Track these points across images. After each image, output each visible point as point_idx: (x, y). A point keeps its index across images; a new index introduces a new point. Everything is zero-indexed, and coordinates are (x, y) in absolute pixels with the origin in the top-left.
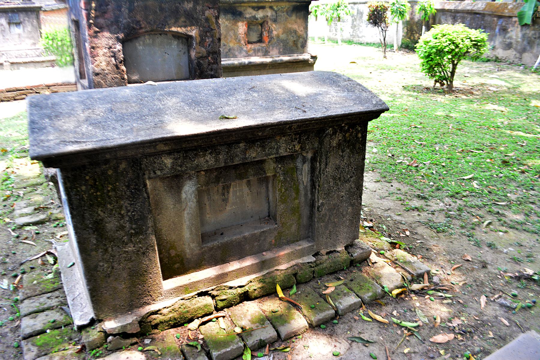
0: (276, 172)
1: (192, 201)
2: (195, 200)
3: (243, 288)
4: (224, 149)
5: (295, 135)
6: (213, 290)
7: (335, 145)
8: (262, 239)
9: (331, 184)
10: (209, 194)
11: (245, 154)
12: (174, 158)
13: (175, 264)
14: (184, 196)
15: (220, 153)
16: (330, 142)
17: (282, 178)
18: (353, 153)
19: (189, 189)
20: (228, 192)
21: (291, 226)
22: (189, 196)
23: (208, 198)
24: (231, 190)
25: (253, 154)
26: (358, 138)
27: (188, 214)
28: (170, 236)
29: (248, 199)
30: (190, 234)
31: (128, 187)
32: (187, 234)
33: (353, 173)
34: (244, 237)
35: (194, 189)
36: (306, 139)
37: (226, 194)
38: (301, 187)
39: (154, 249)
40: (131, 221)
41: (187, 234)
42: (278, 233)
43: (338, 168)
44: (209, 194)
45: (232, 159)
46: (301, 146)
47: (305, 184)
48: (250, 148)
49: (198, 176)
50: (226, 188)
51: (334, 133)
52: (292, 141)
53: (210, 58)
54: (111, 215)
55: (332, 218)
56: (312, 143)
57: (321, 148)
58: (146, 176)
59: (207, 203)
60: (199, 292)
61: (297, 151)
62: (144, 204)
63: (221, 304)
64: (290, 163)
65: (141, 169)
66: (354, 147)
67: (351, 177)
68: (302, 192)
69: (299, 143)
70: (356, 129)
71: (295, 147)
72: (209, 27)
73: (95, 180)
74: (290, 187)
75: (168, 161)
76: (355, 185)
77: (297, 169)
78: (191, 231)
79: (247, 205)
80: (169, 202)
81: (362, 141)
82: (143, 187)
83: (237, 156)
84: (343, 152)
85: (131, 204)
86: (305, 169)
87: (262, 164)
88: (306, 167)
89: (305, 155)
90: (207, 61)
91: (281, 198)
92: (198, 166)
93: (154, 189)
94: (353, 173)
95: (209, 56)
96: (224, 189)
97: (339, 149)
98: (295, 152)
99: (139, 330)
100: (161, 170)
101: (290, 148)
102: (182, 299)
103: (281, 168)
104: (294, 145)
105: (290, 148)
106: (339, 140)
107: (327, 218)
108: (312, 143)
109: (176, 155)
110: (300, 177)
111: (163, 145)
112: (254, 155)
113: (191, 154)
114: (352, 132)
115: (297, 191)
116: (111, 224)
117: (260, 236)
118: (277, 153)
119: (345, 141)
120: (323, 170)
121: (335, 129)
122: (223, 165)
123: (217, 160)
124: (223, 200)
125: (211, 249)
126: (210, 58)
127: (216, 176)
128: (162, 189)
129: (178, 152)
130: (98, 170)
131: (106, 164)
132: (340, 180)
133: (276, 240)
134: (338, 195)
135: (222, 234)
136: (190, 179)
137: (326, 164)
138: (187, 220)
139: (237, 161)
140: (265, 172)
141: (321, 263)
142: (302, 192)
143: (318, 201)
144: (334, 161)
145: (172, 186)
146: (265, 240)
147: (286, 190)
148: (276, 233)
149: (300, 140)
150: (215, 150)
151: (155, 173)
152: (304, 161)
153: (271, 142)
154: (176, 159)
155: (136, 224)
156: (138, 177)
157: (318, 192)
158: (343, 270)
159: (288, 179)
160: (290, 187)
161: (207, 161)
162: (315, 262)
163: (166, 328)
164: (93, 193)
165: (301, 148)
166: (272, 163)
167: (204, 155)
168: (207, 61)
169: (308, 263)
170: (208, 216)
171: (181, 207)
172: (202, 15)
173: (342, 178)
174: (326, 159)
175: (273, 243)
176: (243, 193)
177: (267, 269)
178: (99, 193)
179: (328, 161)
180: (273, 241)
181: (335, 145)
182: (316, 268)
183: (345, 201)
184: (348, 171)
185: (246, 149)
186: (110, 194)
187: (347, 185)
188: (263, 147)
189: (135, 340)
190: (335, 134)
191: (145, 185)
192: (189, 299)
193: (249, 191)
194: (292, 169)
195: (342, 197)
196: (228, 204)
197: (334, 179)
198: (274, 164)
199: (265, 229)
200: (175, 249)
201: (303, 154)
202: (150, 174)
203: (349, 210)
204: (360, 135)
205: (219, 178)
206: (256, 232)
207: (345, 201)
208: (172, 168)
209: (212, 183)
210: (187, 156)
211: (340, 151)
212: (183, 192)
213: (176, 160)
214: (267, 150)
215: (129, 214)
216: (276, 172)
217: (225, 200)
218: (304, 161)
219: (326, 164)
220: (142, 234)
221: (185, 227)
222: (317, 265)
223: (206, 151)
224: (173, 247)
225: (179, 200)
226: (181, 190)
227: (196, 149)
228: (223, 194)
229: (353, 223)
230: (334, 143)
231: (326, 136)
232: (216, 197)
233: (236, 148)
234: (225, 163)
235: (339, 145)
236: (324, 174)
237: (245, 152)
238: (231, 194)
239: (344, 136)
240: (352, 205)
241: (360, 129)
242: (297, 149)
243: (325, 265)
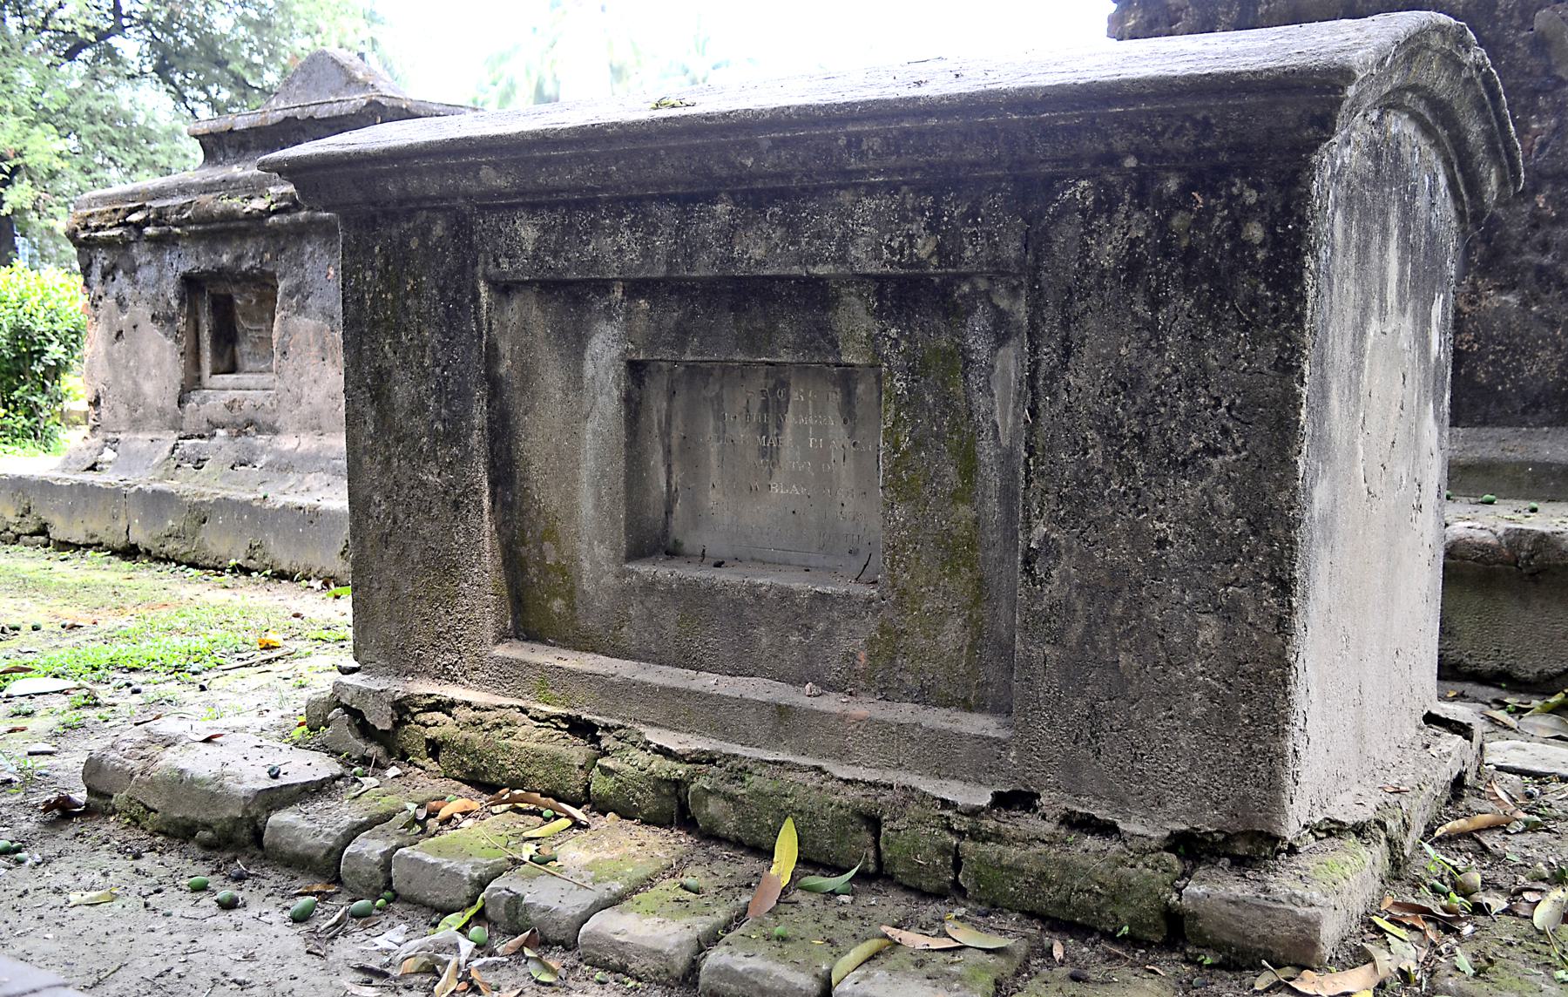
0: (877, 353)
1: (608, 394)
2: (616, 393)
3: (669, 764)
4: (666, 213)
5: (917, 193)
6: (607, 728)
7: (1107, 263)
8: (821, 627)
9: (1095, 456)
10: (720, 417)
11: (730, 244)
12: (542, 226)
13: (555, 595)
14: (589, 369)
15: (656, 227)
16: (1086, 249)
17: (900, 386)
18: (1217, 321)
19: (605, 349)
20: (779, 427)
21: (941, 616)
22: (602, 373)
23: (716, 430)
24: (790, 419)
25: (760, 250)
26: (1247, 245)
27: (594, 433)
28: (542, 489)
29: (845, 472)
30: (597, 507)
31: (442, 290)
32: (586, 505)
33: (1225, 432)
34: (752, 589)
35: (615, 352)
36: (964, 217)
37: (773, 431)
38: (987, 451)
39: (481, 501)
40: (440, 391)
41: (586, 505)
42: (883, 630)
43: (1128, 384)
44: (720, 417)
45: (691, 256)
46: (939, 246)
47: (1005, 442)
48: (747, 225)
49: (629, 311)
50: (774, 406)
51: (1106, 204)
52: (904, 219)
53: (1541, 200)
54: (406, 364)
55: (1104, 640)
56: (990, 235)
57: (1038, 268)
58: (480, 269)
59: (714, 447)
60: (572, 712)
61: (921, 263)
62: (470, 351)
63: (601, 786)
64: (938, 332)
65: (470, 246)
66: (1223, 293)
67: (1216, 452)
68: (992, 478)
69: (932, 228)
70: (1231, 197)
71: (912, 246)
72: (1547, 71)
73: (387, 263)
74: (937, 436)
75: (528, 233)
76: (1236, 499)
77: (968, 362)
78: (599, 498)
79: (841, 497)
80: (552, 378)
81: (1269, 262)
82: (471, 301)
83: (705, 246)
84: (1155, 304)
85: (444, 345)
86: (1005, 371)
87: (825, 309)
88: (1010, 363)
89: (1004, 304)
90: (1526, 209)
91: (893, 471)
92: (595, 260)
93: (524, 327)
94: (1225, 432)
95: (1536, 190)
96: (765, 407)
97: (1131, 281)
98: (912, 266)
99: (388, 726)
100: (511, 257)
101: (895, 244)
102: (524, 711)
103: (896, 343)
104: (911, 237)
105: (895, 244)
106: (1133, 243)
107: (1078, 629)
108: (990, 235)
109: (547, 217)
110: (980, 401)
111: (492, 173)
112: (758, 253)
113: (582, 219)
114: (1209, 211)
115: (969, 465)
116: (402, 393)
117: (810, 609)
118: (842, 260)
119: (1165, 250)
120: (1051, 377)
121: (1109, 187)
122: (661, 271)
123: (647, 253)
124: (764, 452)
125: (649, 587)
126: (1541, 200)
127: (678, 324)
128: (540, 333)
129: (552, 207)
130: (395, 232)
131: (409, 221)
132: (1144, 451)
133: (870, 657)
134: (1135, 532)
135: (718, 565)
136: (610, 318)
137: (1068, 352)
138: (590, 455)
139: (704, 267)
140: (834, 343)
141: (998, 837)
142: (992, 478)
143: (1029, 528)
144: (1105, 345)
145: (562, 329)
146: (828, 634)
147: (918, 444)
148: (873, 623)
149: (938, 216)
150: (645, 216)
151: (498, 265)
152: (1001, 331)
153: (821, 212)
154: (546, 230)
155: (448, 405)
156: (462, 269)
157: (1028, 481)
158: (1111, 937)
159: (930, 399)
160: (937, 436)
161: (620, 250)
162: (974, 812)
163: (456, 772)
164: (380, 292)
165: (940, 250)
166: (862, 313)
167: (615, 230)
168: (1526, 209)
169: (945, 804)
170: (712, 494)
171: (580, 403)
172: (1519, 29)
173: (1155, 441)
174: (1065, 324)
175: (860, 666)
176: (827, 443)
177: (793, 752)
178: (390, 296)
179: (1075, 336)
180: (862, 655)
181: (1107, 263)
182: (968, 845)
183: (1176, 572)
184: (1191, 414)
185: (735, 227)
186: (409, 302)
187: (1190, 491)
188: (792, 229)
189: (374, 750)
190: (1111, 212)
191: (476, 297)
192: (537, 719)
193: (848, 443)
194: (947, 356)
195: (1161, 543)
196: (776, 470)
197: (1112, 435)
198: (870, 320)
199: (829, 589)
200: (557, 542)
201: (996, 300)
202: (487, 263)
203: (1205, 635)
204: (1255, 232)
205: (686, 333)
206: (795, 586)
207: (1176, 572)
208: (535, 257)
209: (665, 344)
210: (571, 225)
211: (1139, 297)
212: (587, 356)
213: (545, 232)
214: (804, 241)
215: (438, 370)
216: (877, 353)
217: (770, 454)
218: (1001, 331)
219: (1068, 352)
220: (456, 442)
221: (584, 475)
222: (976, 835)
223: (621, 215)
224: (550, 534)
225: (576, 382)
226: (585, 347)
227: (589, 203)
228: (764, 430)
229: (1230, 718)
230: (1106, 254)
231: (1059, 215)
232: (742, 434)
233: (704, 220)
234: (669, 264)
235: (1132, 268)
236: (1055, 395)
237: (728, 234)
238: (788, 437)
239: (1162, 226)
240: (1229, 612)
241: (1251, 197)
242: (923, 254)
243: (1013, 853)
